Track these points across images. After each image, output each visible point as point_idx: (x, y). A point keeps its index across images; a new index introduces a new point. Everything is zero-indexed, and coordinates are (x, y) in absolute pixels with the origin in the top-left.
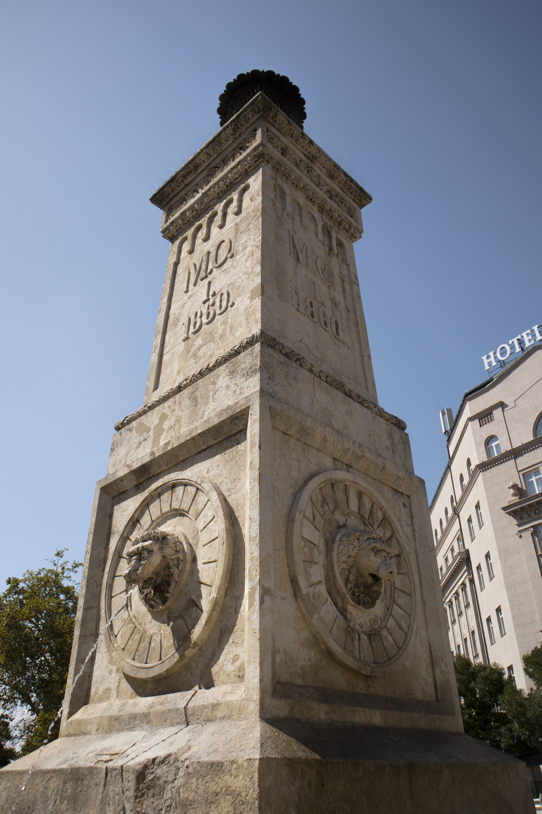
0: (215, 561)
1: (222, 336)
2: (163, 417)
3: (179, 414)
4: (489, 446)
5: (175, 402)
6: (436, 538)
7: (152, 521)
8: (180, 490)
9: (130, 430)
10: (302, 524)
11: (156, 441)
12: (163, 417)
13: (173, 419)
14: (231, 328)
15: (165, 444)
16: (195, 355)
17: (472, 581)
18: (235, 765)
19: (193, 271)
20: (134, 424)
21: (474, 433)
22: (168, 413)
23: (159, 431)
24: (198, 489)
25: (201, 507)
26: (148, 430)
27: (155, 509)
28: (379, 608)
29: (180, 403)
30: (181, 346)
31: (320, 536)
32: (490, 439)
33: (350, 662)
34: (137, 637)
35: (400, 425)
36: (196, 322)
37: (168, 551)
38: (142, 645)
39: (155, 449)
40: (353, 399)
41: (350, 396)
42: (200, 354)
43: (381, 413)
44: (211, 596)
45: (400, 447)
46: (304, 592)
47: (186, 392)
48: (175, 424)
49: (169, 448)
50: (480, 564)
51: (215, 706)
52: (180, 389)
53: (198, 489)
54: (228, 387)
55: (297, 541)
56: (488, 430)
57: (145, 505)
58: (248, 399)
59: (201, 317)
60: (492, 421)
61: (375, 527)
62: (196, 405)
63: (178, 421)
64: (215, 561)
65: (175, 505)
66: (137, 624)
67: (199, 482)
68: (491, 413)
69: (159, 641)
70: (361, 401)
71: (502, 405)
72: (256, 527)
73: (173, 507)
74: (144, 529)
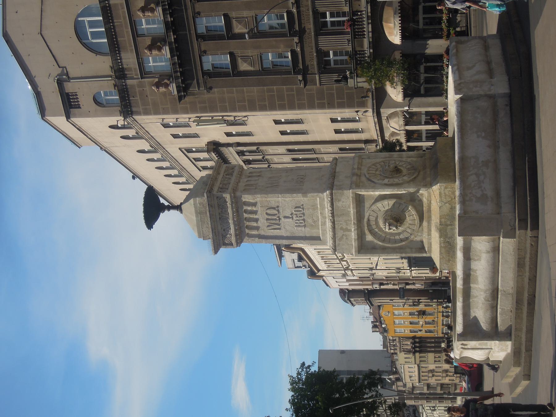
4: (105, 103)
17: (239, 144)
19: (271, 228)
21: (87, 115)
25: (378, 209)
28: (402, 168)
30: (307, 229)
32: (97, 101)
33: (417, 174)
36: (300, 223)
37: (389, 218)
50: (225, 133)
51: (428, 201)
55: (389, 183)
56: (85, 100)
58: (353, 193)
59: (299, 220)
60: (76, 95)
65: (374, 219)
68: (68, 94)
71: (60, 83)
72: (389, 190)
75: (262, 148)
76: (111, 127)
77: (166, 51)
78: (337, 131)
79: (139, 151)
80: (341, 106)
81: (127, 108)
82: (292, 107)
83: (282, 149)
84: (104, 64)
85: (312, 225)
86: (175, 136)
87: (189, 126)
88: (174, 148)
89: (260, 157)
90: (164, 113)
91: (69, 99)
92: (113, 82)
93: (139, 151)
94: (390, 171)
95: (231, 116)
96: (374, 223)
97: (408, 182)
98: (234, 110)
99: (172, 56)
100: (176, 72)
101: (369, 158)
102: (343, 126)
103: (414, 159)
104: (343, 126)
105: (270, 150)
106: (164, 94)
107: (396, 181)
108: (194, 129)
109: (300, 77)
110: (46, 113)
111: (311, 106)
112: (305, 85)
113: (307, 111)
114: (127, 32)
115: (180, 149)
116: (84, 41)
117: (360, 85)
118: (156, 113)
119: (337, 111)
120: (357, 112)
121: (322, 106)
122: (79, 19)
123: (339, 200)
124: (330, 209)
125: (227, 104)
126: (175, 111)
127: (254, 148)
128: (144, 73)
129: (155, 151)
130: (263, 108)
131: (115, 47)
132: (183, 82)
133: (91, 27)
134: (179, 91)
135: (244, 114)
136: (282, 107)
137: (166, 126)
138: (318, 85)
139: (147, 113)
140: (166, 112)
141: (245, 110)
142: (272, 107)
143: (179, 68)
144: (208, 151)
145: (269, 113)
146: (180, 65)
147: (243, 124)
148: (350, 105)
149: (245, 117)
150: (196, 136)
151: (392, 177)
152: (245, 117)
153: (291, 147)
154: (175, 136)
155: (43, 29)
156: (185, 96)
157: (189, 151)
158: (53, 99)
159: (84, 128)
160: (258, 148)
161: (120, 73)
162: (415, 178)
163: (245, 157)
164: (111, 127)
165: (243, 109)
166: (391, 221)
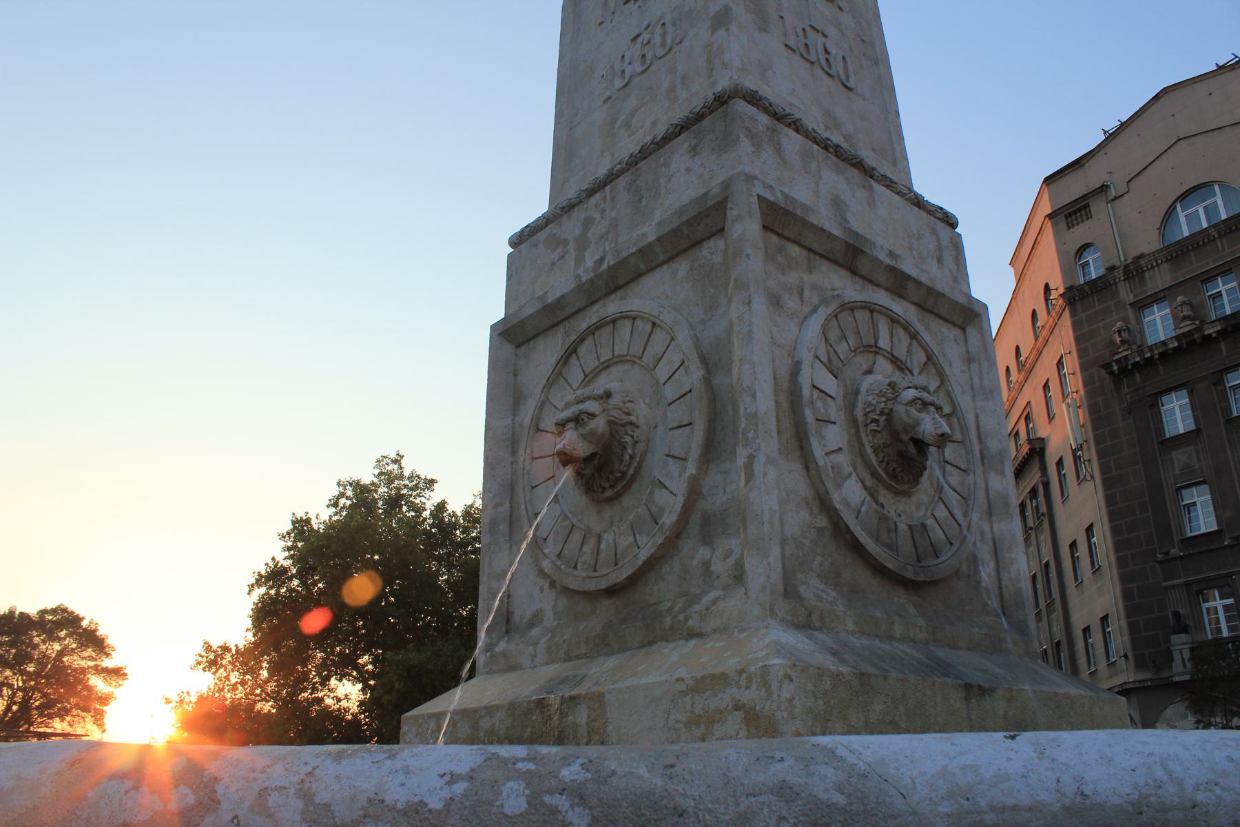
0: (690, 424)
1: (672, 89)
2: (589, 222)
3: (613, 215)
5: (605, 198)
6: (1009, 382)
7: (586, 376)
8: (625, 327)
9: (536, 245)
10: (812, 367)
11: (579, 260)
12: (589, 222)
13: (604, 223)
14: (684, 79)
15: (596, 262)
16: (627, 125)
17: (1046, 485)
18: (745, 675)
20: (542, 236)
22: (597, 216)
23: (582, 243)
24: (654, 324)
26: (565, 243)
27: (588, 356)
29: (613, 199)
31: (838, 386)
34: (576, 538)
35: (950, 221)
38: (585, 549)
39: (580, 271)
40: (877, 181)
41: (872, 177)
42: (634, 121)
43: (918, 202)
44: (688, 473)
45: (948, 256)
46: (821, 463)
47: (622, 181)
48: (608, 232)
49: (604, 267)
52: (611, 177)
53: (654, 324)
54: (688, 170)
56: (1082, 232)
57: (572, 351)
61: (916, 372)
62: (640, 200)
63: (614, 226)
64: (690, 424)
65: (620, 349)
66: (574, 520)
67: (656, 314)
68: (1087, 206)
69: (611, 541)
70: (889, 184)
71: (1104, 188)
73: (616, 353)
74: (575, 386)
75: (1046, 525)
76: (1047, 285)
77: (1187, 326)
78: (1086, 630)
79: (1017, 348)
80: (1133, 628)
81: (1076, 296)
82: (1118, 546)
83: (1047, 555)
84: (1146, 241)
85: (614, 120)
86: (1046, 386)
87: (1064, 396)
88: (1032, 394)
89: (1030, 523)
90: (1079, 351)
91: (1080, 210)
92: (1118, 264)
93: (1017, 348)
94: (889, 414)
95: (1091, 453)
96: (606, 355)
97: (824, 504)
98: (1101, 454)
99: (1177, 338)
100: (1151, 348)
101: (969, 359)
102: (1096, 638)
103: (987, 574)
104: (1096, 638)
105: (1045, 537)
106: (1112, 343)
107: (831, 441)
108: (1061, 409)
109: (1174, 552)
110: (1053, 186)
111: (1125, 578)
112: (1159, 562)
113: (1115, 573)
114: (1208, 264)
115: (1029, 403)
116: (1178, 206)
117: (1177, 656)
118: (1078, 340)
119: (1124, 622)
120: (1126, 656)
121: (1127, 595)
122: (1216, 187)
123: (694, 151)
124: (660, 131)
125: (1109, 443)
126: (1084, 367)
127: (1043, 509)
128: (1142, 305)
129: (1021, 366)
130: (1110, 500)
131: (1178, 252)
132: (1136, 365)
133: (1205, 208)
134: (1118, 361)
135: (1097, 474)
136: (1115, 531)
137: (1060, 364)
138: (1165, 584)
139: (1076, 326)
140: (1082, 353)
141: (1103, 473)
142: (1114, 515)
143: (1160, 354)
144: (1029, 441)
145: (1104, 511)
146: (1164, 355)
147: (1080, 480)
148: (1135, 643)
149: (1092, 476)
150: (1051, 418)
151: (853, 422)
152: (1092, 476)
153: (1052, 565)
154: (1046, 386)
155: (1187, 141)
156: (1111, 373)
157: (1028, 419)
158: (1075, 188)
159: (1038, 250)
160: (1043, 515)
161: (1134, 270)
162: (857, 548)
163: (1028, 501)
164: (1047, 285)
165: (1104, 470)
166: (599, 424)
